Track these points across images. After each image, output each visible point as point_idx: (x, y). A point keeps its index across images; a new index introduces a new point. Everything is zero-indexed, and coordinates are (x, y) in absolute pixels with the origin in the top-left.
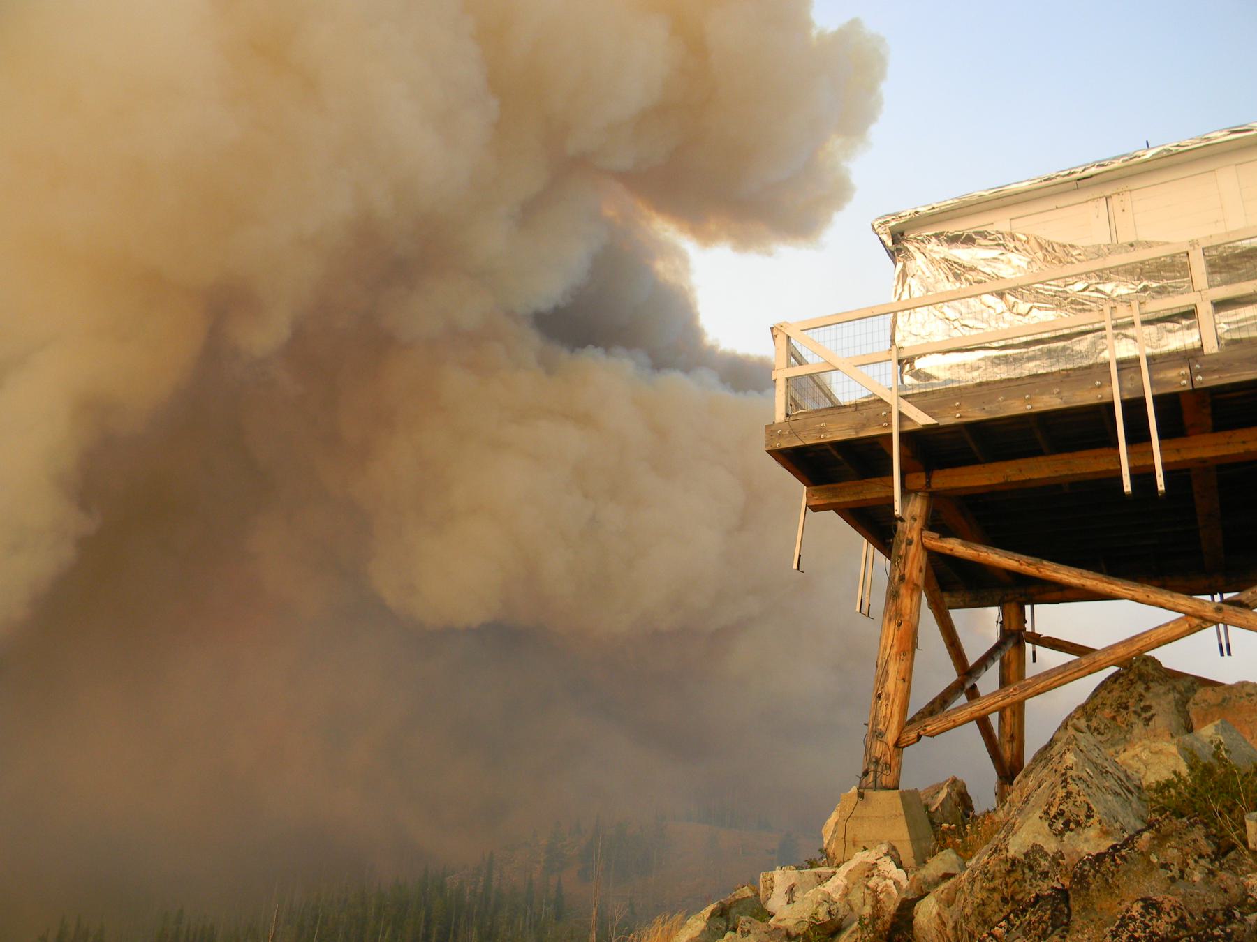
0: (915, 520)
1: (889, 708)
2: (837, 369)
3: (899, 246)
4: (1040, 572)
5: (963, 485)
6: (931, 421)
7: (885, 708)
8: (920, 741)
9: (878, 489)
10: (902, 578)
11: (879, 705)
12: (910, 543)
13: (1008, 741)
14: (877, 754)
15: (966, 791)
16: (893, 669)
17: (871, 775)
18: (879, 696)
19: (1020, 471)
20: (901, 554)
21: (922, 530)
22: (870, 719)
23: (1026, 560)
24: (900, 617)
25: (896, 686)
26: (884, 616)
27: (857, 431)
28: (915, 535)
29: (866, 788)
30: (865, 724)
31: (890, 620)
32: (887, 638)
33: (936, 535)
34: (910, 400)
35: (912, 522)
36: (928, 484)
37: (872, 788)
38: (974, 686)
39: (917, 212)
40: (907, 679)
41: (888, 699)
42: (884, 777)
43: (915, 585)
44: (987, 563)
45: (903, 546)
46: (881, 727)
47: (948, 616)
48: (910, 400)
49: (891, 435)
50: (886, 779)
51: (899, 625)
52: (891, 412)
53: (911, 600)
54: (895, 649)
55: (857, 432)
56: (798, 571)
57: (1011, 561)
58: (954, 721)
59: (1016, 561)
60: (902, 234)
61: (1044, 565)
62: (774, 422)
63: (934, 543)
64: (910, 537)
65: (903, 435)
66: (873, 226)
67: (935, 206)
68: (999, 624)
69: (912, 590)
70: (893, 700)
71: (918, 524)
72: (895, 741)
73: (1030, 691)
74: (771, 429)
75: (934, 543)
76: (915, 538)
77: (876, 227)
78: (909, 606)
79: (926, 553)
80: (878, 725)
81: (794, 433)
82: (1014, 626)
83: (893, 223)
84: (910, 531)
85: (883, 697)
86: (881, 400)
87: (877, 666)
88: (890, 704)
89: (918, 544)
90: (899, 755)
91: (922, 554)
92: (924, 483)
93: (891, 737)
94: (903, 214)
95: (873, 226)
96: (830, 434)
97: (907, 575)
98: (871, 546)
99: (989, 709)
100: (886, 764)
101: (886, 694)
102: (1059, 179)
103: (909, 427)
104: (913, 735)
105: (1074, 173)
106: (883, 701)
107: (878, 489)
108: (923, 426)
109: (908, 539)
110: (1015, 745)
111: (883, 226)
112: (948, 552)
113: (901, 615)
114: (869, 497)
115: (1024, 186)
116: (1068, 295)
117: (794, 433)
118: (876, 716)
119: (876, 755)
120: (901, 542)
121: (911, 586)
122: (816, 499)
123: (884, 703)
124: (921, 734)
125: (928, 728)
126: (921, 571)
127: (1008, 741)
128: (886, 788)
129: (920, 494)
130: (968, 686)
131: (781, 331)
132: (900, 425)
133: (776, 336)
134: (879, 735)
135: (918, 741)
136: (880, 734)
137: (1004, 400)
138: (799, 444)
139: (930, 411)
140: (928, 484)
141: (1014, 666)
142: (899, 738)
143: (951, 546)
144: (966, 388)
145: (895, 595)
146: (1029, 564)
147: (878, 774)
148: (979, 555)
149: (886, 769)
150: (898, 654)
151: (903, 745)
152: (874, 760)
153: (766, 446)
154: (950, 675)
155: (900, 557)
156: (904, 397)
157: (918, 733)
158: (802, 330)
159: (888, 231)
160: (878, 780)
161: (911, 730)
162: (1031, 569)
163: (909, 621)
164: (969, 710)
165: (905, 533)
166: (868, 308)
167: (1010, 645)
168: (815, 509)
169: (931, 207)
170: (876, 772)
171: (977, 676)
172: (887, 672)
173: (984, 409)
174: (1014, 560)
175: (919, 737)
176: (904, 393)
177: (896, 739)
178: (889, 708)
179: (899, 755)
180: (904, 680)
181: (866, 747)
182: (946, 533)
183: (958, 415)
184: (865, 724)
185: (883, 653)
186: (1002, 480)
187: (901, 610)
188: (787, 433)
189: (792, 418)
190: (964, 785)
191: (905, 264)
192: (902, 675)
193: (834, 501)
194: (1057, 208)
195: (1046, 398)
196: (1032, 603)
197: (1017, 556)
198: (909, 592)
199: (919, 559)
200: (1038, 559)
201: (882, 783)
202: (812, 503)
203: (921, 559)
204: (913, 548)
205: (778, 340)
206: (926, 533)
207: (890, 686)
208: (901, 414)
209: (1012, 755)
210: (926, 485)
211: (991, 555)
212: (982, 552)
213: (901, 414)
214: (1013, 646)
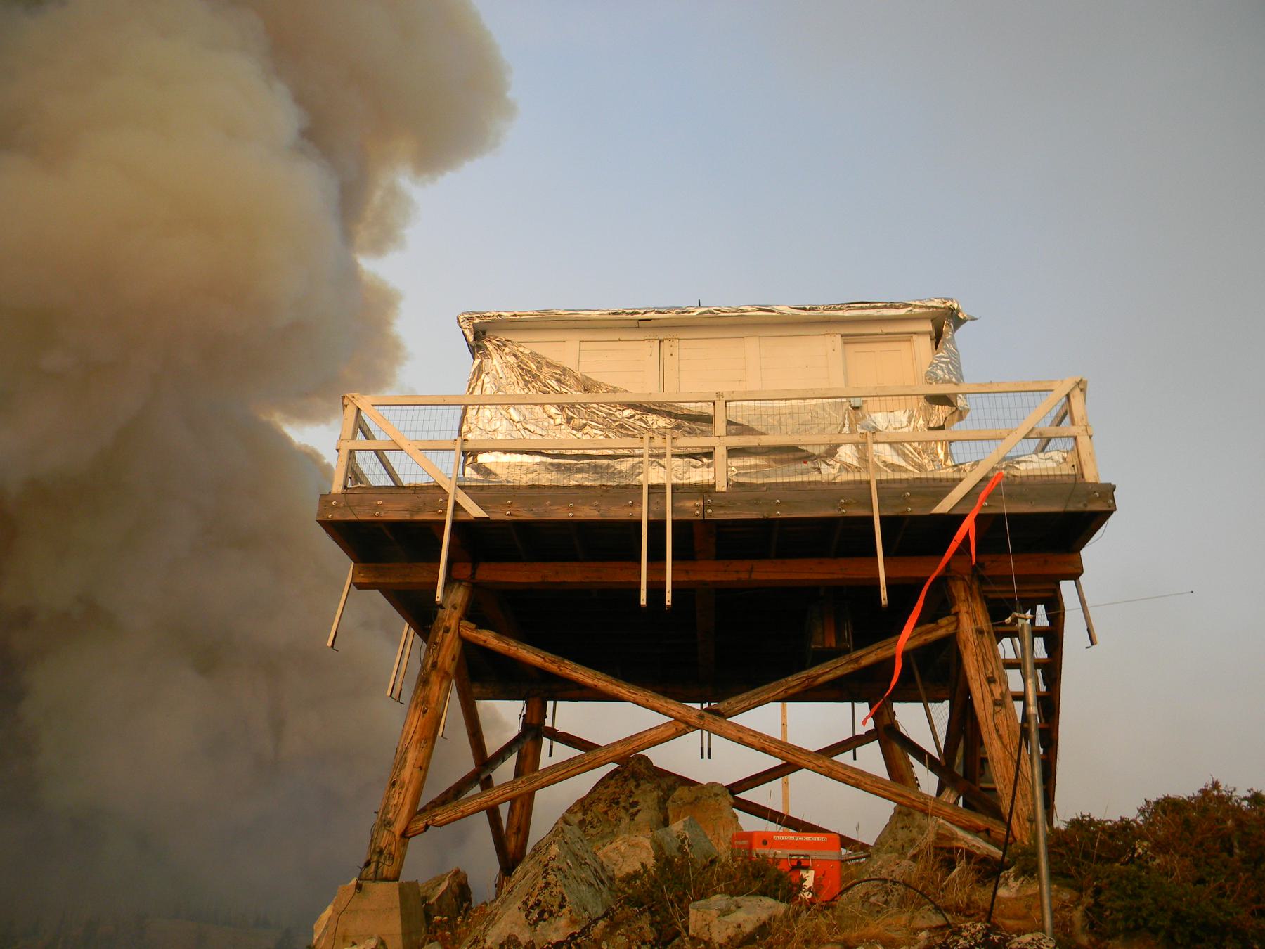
0: (455, 608)
1: (402, 796)
2: (402, 450)
3: (480, 344)
4: (561, 670)
5: (504, 580)
6: (483, 514)
7: (397, 796)
8: (428, 831)
9: (425, 574)
10: (434, 665)
11: (392, 792)
12: (447, 630)
13: (515, 833)
14: (382, 845)
15: (467, 882)
16: (411, 756)
17: (373, 866)
18: (394, 784)
19: (557, 573)
20: (437, 640)
21: (460, 619)
22: (379, 808)
23: (550, 658)
24: (427, 703)
25: (412, 774)
26: (412, 702)
27: (412, 513)
28: (453, 623)
29: (365, 880)
30: (375, 812)
31: (416, 706)
32: (411, 724)
33: (473, 626)
34: (467, 491)
35: (453, 610)
36: (473, 574)
37: (371, 880)
38: (489, 777)
39: (500, 316)
40: (424, 768)
41: (402, 787)
42: (386, 868)
43: (446, 673)
44: (515, 657)
45: (441, 633)
46: (390, 815)
47: (474, 706)
48: (467, 491)
49: (444, 522)
50: (387, 870)
51: (425, 712)
52: (447, 500)
53: (440, 688)
54: (416, 737)
55: (412, 515)
56: (331, 649)
57: (537, 657)
58: (463, 811)
59: (542, 657)
60: (484, 333)
61: (565, 664)
62: (330, 493)
63: (470, 633)
64: (448, 625)
65: (455, 524)
66: (458, 319)
67: (517, 313)
68: (522, 718)
69: (443, 678)
70: (407, 789)
71: (457, 613)
72: (402, 830)
73: (537, 784)
74: (325, 499)
75: (470, 633)
76: (453, 627)
77: (461, 320)
78: (437, 694)
79: (461, 643)
80: (388, 813)
81: (349, 506)
82: (535, 722)
83: (477, 321)
84: (449, 619)
85: (398, 784)
86: (439, 487)
87: (397, 752)
88: (403, 792)
89: (455, 632)
90: (404, 845)
91: (457, 643)
92: (469, 573)
93: (398, 827)
94: (488, 314)
95: (458, 319)
96: (385, 513)
97: (439, 664)
98: (412, 631)
99: (497, 800)
100: (390, 854)
101: (401, 782)
102: (624, 316)
103: (462, 517)
104: (421, 825)
105: (638, 313)
106: (397, 789)
107: (425, 574)
108: (475, 518)
109: (446, 627)
110: (520, 836)
111: (468, 321)
112: (481, 643)
113: (428, 702)
114: (415, 580)
115: (595, 314)
116: (617, 419)
117: (349, 506)
118: (387, 804)
119: (382, 845)
120: (439, 629)
121: (442, 674)
122: (363, 577)
123: (397, 792)
124: (429, 824)
125: (437, 818)
126: (453, 660)
127: (515, 833)
128: (386, 879)
129: (464, 583)
130: (483, 777)
131: (352, 401)
132: (454, 515)
133: (346, 406)
134: (388, 824)
135: (425, 831)
136: (389, 823)
137: (550, 505)
138: (353, 518)
139: (484, 505)
140: (473, 574)
141: (530, 759)
142: (407, 828)
143: (484, 638)
144: (519, 488)
145: (424, 682)
146: (553, 662)
147: (381, 864)
148: (509, 649)
149: (389, 860)
150: (419, 741)
151: (410, 835)
152: (378, 850)
153: (318, 515)
154: (467, 764)
155: (436, 644)
156: (461, 487)
157: (427, 823)
158: (373, 405)
159: (471, 327)
160: (380, 871)
161: (419, 820)
162: (553, 667)
163: (435, 709)
164: (478, 800)
165: (444, 621)
166: (442, 396)
167: (528, 739)
168: (360, 586)
169: (513, 314)
170: (378, 862)
171: (493, 767)
172: (405, 758)
173: (532, 510)
174: (539, 656)
175: (427, 827)
176: (463, 484)
177: (404, 828)
178: (402, 796)
179: (405, 845)
180: (421, 768)
181: (372, 836)
182: (482, 624)
183: (508, 513)
184: (375, 812)
185: (405, 740)
186: (539, 580)
187: (429, 696)
188: (341, 505)
189: (349, 491)
190: (466, 877)
191: (481, 362)
192: (419, 763)
193: (380, 580)
194: (620, 340)
195: (587, 509)
196: (555, 700)
197: (543, 653)
198: (439, 679)
199: (453, 648)
200: (560, 658)
201: (382, 874)
202: (358, 580)
203: (456, 645)
204: (449, 636)
205: (347, 410)
206: (464, 623)
207: (406, 773)
208: (456, 504)
209: (516, 846)
210: (471, 575)
211: (521, 650)
212: (512, 646)
213: (456, 504)
214: (530, 740)
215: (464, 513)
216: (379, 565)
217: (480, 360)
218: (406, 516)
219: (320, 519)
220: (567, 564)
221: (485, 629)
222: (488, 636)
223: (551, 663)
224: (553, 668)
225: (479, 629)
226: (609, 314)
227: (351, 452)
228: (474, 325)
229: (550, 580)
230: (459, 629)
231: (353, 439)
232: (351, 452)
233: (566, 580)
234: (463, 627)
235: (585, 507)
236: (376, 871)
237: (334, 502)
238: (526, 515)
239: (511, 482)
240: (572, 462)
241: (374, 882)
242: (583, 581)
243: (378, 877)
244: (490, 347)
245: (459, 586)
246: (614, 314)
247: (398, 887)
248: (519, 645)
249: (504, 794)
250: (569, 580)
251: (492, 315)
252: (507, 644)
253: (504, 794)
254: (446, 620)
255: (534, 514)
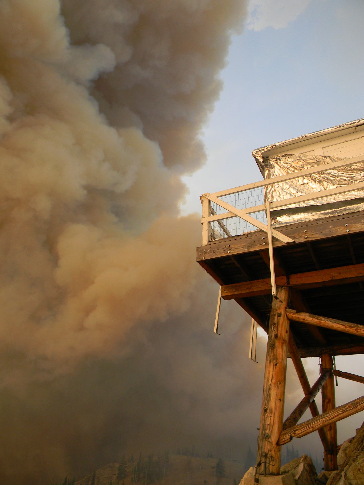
0: (282, 302)
1: (272, 418)
2: (236, 216)
3: (266, 163)
4: (357, 332)
5: (308, 282)
6: (291, 240)
7: (269, 418)
8: (291, 442)
9: (260, 286)
10: (276, 336)
11: (266, 417)
12: (279, 315)
13: (329, 430)
14: (266, 451)
15: (312, 463)
16: (273, 393)
17: (263, 465)
18: (266, 411)
19: (340, 273)
20: (275, 322)
21: (286, 308)
22: (260, 426)
23: (348, 325)
24: (276, 359)
25: (275, 403)
26: (266, 359)
27: (248, 247)
28: (282, 311)
29: (261, 474)
30: (258, 429)
31: (270, 362)
32: (269, 373)
33: (294, 311)
34: (278, 230)
35: (280, 303)
36: (288, 282)
37: (263, 474)
38: (314, 401)
39: (275, 146)
40: (282, 400)
41: (271, 413)
42: (271, 466)
43: (284, 340)
44: (325, 327)
45: (276, 317)
46: (267, 431)
47: (300, 361)
48: (278, 230)
49: (268, 249)
50: (272, 468)
51: (276, 365)
52: (267, 237)
53: (282, 350)
54: (274, 381)
55: (248, 249)
56: (217, 334)
57: (339, 325)
58: (313, 427)
59: (343, 325)
60: (267, 158)
61: (359, 327)
62: (202, 246)
63: (294, 316)
64: (279, 312)
65: (275, 250)
66: (253, 154)
67: (284, 142)
68: (320, 365)
69: (283, 344)
70: (274, 414)
71: (284, 305)
72: (276, 441)
73: (359, 407)
74: (200, 249)
75: (294, 316)
76: (283, 313)
77: (254, 153)
78: (281, 353)
79: (289, 322)
80: (266, 430)
81: (213, 251)
82: (328, 367)
83: (263, 151)
84: (279, 308)
85: (268, 411)
86: (262, 231)
87: (264, 391)
88: (272, 416)
89: (284, 316)
90: (279, 450)
91: (287, 322)
92: (286, 282)
93: (274, 438)
94: (267, 147)
95: (253, 154)
96: (233, 250)
97: (279, 335)
98: (256, 323)
99: (334, 419)
100: (272, 457)
101: (270, 409)
102: (346, 126)
103: (278, 245)
104: (287, 437)
105: (356, 123)
106: (268, 414)
107: (260, 286)
108: (286, 243)
109: (278, 313)
110: (332, 432)
111: (258, 153)
112: (302, 321)
113: (277, 359)
114: (255, 290)
115: (329, 130)
116: (357, 179)
117: (213, 251)
118: (264, 425)
119: (265, 451)
120: (275, 315)
121: (282, 341)
122: (226, 292)
123: (269, 416)
124: (292, 436)
125: (297, 432)
126: (286, 332)
127: (329, 430)
128: (272, 474)
129: (284, 287)
130: (311, 401)
131: (205, 198)
132: (273, 244)
133: (203, 201)
134: (267, 437)
135: (290, 441)
136: (267, 436)
137: (333, 228)
138: (216, 256)
139: (290, 235)
140: (288, 282)
141: (329, 388)
142: (279, 439)
143: (303, 317)
144: (309, 222)
145: (272, 347)
146: (351, 327)
147: (267, 465)
148: (320, 322)
149: (272, 461)
150: (276, 383)
151: (282, 443)
152: (264, 454)
153: (197, 258)
154: (302, 396)
155: (275, 324)
156: (275, 229)
157: (291, 435)
158: (218, 197)
159: (260, 154)
160: (267, 469)
161: (286, 434)
162: (352, 330)
163: (281, 362)
164: (322, 420)
165: (277, 310)
166: (253, 183)
167: (327, 377)
168: (226, 298)
169: (281, 143)
170: (265, 463)
171: (315, 395)
172: (270, 394)
173: (321, 233)
174: (341, 324)
175: (291, 438)
176: (274, 227)
177: (277, 439)
178: (272, 418)
179: (279, 450)
180: (280, 400)
181: (259, 445)
182: (299, 311)
183: (306, 237)
184: (258, 429)
185: (267, 383)
186: (329, 279)
187: (276, 355)
188: (209, 251)
189: (211, 243)
190: (311, 460)
191: (269, 172)
192: (279, 397)
193: (236, 293)
194: (346, 141)
195: (358, 225)
196: (334, 356)
197: (343, 323)
198: (281, 344)
199: (285, 326)
200: (355, 324)
201: (269, 471)
202: (224, 295)
203: (286, 324)
204: (281, 319)
205: (204, 203)
206: (288, 310)
207: (272, 404)
208: (273, 238)
209: (331, 437)
210: (287, 282)
211: (328, 322)
212: (322, 320)
213: (273, 238)
214: (329, 377)
215: (278, 242)
216: (235, 285)
217: (268, 171)
218: (245, 250)
219: (199, 260)
220: (345, 267)
221: (302, 312)
222: (305, 316)
223: (350, 328)
224: (352, 331)
225: (299, 312)
226: (337, 128)
227: (209, 223)
228: (262, 154)
229: (336, 278)
230: (286, 314)
231: (209, 216)
232: (209, 223)
233: (346, 277)
234: (289, 313)
235: (356, 225)
236: (265, 470)
237: (205, 250)
238: (317, 236)
239: (303, 220)
240: (333, 210)
241: (265, 476)
242: (358, 275)
243: (267, 473)
244: (272, 163)
245: (282, 289)
246: (340, 127)
247: (281, 480)
248: (326, 319)
249: (338, 415)
250: (349, 277)
251: (270, 146)
252: (319, 319)
253: (338, 415)
254: (278, 309)
255: (323, 235)
